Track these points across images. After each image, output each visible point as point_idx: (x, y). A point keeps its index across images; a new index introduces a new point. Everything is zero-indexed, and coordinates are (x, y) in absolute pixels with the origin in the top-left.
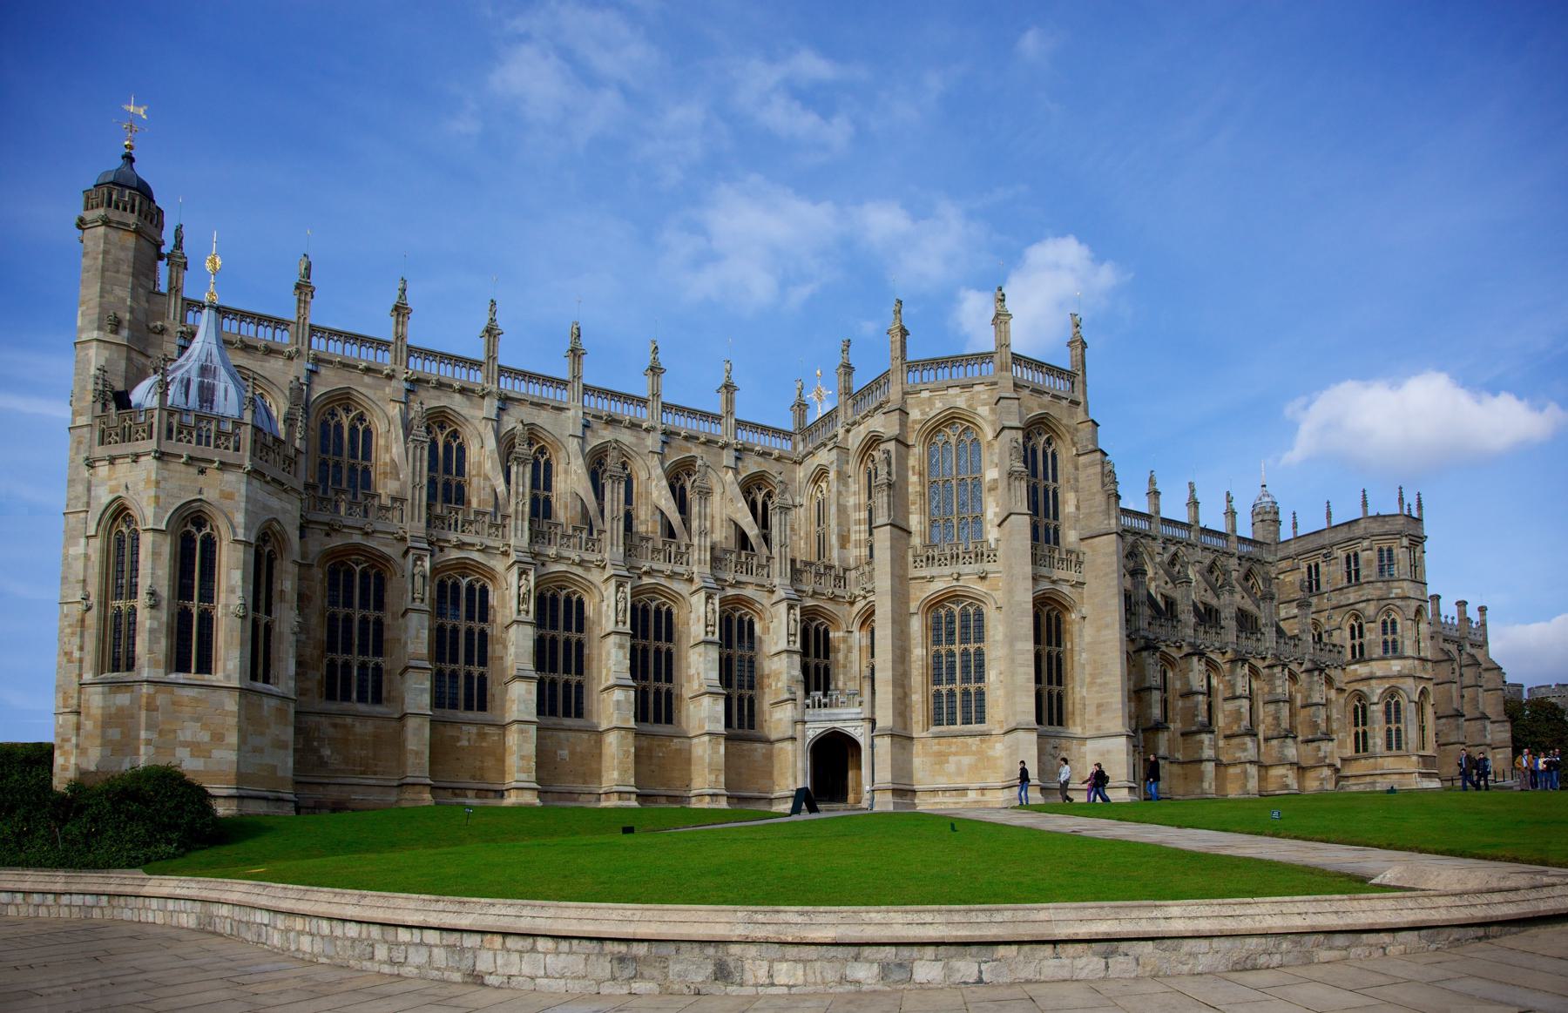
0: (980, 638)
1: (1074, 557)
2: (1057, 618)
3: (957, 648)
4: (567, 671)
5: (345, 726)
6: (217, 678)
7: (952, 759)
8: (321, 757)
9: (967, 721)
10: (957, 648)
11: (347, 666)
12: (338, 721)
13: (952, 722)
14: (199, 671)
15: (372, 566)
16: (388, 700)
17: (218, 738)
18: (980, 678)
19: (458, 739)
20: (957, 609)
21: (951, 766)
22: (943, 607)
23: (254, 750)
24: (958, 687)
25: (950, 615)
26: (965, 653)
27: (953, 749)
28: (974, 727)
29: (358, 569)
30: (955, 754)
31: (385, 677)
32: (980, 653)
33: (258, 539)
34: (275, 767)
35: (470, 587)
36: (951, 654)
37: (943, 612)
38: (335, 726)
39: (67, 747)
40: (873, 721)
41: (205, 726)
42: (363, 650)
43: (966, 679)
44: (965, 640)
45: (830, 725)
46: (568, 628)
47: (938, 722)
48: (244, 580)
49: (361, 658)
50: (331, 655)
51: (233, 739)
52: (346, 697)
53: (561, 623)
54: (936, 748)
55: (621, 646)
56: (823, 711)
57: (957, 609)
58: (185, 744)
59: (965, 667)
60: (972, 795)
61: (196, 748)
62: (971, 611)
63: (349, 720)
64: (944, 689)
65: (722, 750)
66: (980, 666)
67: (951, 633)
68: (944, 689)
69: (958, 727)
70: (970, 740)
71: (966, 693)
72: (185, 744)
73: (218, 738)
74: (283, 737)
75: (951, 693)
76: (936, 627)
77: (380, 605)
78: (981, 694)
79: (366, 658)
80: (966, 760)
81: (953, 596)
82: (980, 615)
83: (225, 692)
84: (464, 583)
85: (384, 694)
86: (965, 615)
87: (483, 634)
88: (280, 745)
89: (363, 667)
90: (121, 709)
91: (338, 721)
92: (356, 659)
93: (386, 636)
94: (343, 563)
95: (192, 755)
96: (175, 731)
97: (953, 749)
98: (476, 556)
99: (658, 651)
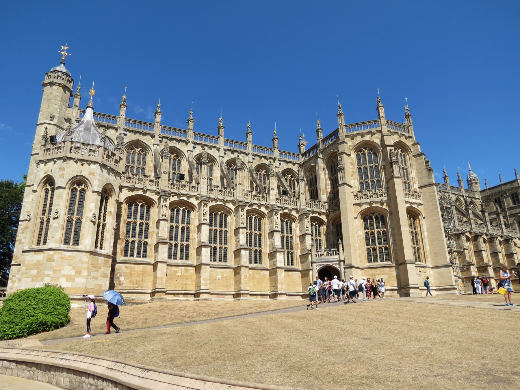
1: (417, 194)
5: (131, 268)
6: (80, 247)
8: (120, 281)
10: (375, 231)
14: (74, 244)
16: (149, 257)
17: (78, 273)
23: (94, 278)
33: (103, 191)
34: (101, 286)
38: (127, 268)
39: (14, 279)
41: (73, 268)
45: (326, 264)
47: (370, 261)
48: (96, 207)
50: (127, 239)
51: (85, 273)
55: (243, 233)
58: (64, 276)
61: (69, 278)
62: (379, 216)
64: (371, 247)
68: (371, 247)
69: (379, 263)
72: (64, 276)
73: (78, 273)
74: (106, 272)
83: (84, 253)
85: (148, 254)
88: (104, 276)
90: (38, 261)
95: (67, 281)
96: (60, 270)
97: (378, 272)
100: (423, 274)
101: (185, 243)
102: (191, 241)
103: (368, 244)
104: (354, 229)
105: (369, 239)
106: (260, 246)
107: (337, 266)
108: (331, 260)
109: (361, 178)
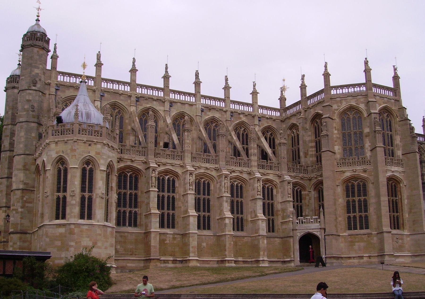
0: (365, 194)
2: (395, 186)
3: (356, 199)
4: (204, 211)
5: (125, 236)
7: (356, 244)
9: (361, 228)
10: (356, 199)
11: (125, 212)
12: (122, 234)
13: (355, 228)
15: (134, 173)
18: (366, 211)
19: (166, 240)
20: (356, 183)
21: (356, 247)
22: (350, 182)
24: (357, 214)
25: (353, 185)
26: (360, 201)
27: (357, 240)
28: (364, 231)
29: (129, 175)
30: (358, 242)
31: (138, 217)
32: (365, 201)
35: (169, 179)
36: (354, 201)
37: (350, 184)
38: (121, 236)
40: (325, 229)
42: (130, 206)
43: (360, 211)
44: (359, 195)
46: (204, 194)
47: (350, 229)
49: (130, 209)
52: (124, 225)
53: (202, 192)
54: (349, 239)
55: (227, 202)
56: (304, 225)
57: (356, 183)
59: (360, 206)
60: (365, 259)
62: (361, 184)
63: (126, 234)
64: (352, 215)
65: (265, 241)
66: (366, 206)
67: (353, 193)
69: (358, 231)
70: (363, 236)
71: (361, 217)
75: (355, 217)
76: (347, 190)
77: (136, 188)
78: (366, 217)
79: (131, 209)
80: (362, 244)
81: (354, 178)
82: (364, 186)
84: (167, 178)
85: (138, 223)
86: (359, 185)
87: (173, 198)
89: (130, 212)
91: (122, 234)
92: (128, 209)
93: (139, 200)
94: (123, 172)
97: (357, 240)
98: (171, 168)
99: (237, 202)
100: (400, 241)
101: (171, 212)
102: (176, 209)
103: (349, 212)
104: (335, 197)
105: (350, 207)
106: (242, 213)
107: (318, 234)
108: (313, 227)
109: (345, 144)
